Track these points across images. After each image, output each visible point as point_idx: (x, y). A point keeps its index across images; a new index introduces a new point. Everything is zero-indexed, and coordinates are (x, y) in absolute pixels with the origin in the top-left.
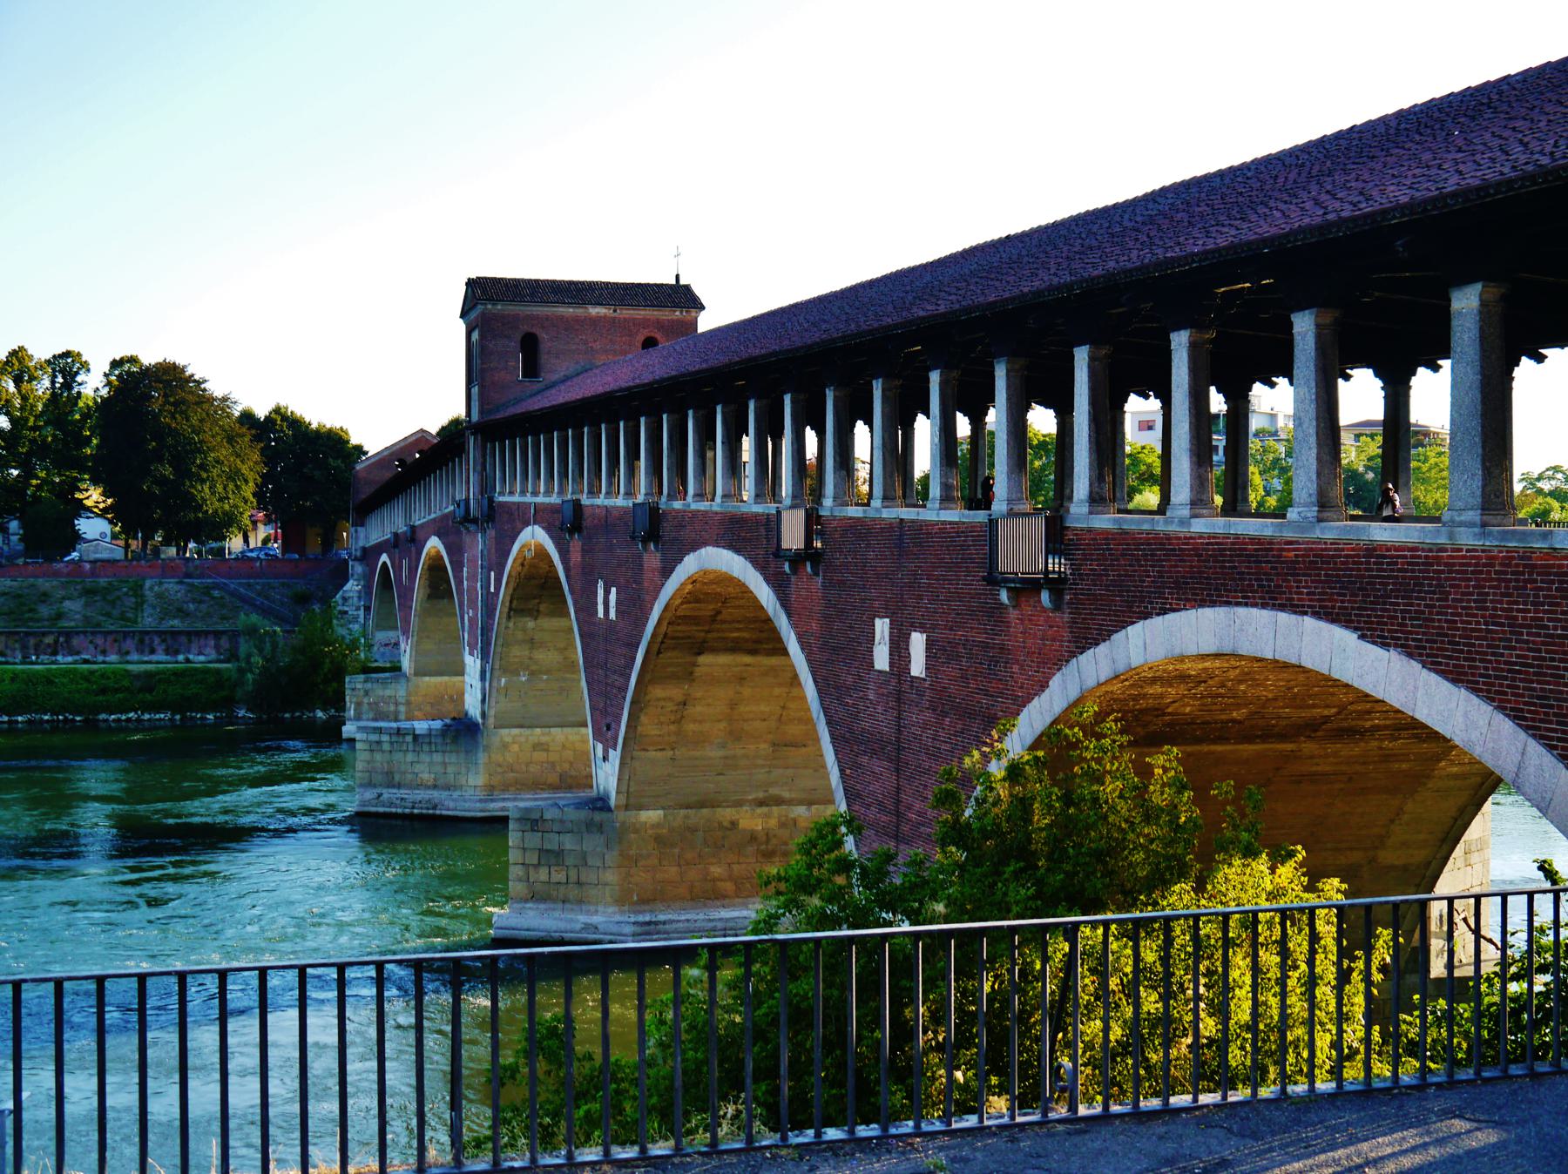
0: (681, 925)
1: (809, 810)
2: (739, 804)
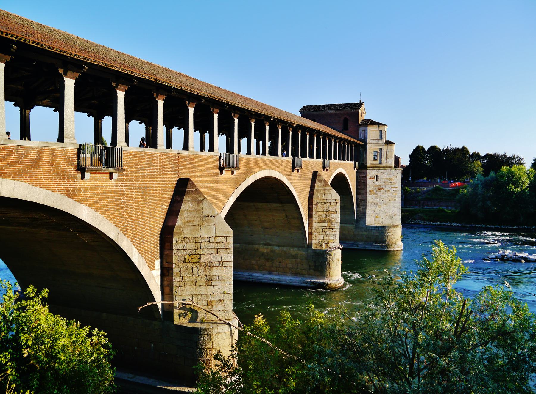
0: (240, 276)
1: (278, 248)
2: (259, 244)
